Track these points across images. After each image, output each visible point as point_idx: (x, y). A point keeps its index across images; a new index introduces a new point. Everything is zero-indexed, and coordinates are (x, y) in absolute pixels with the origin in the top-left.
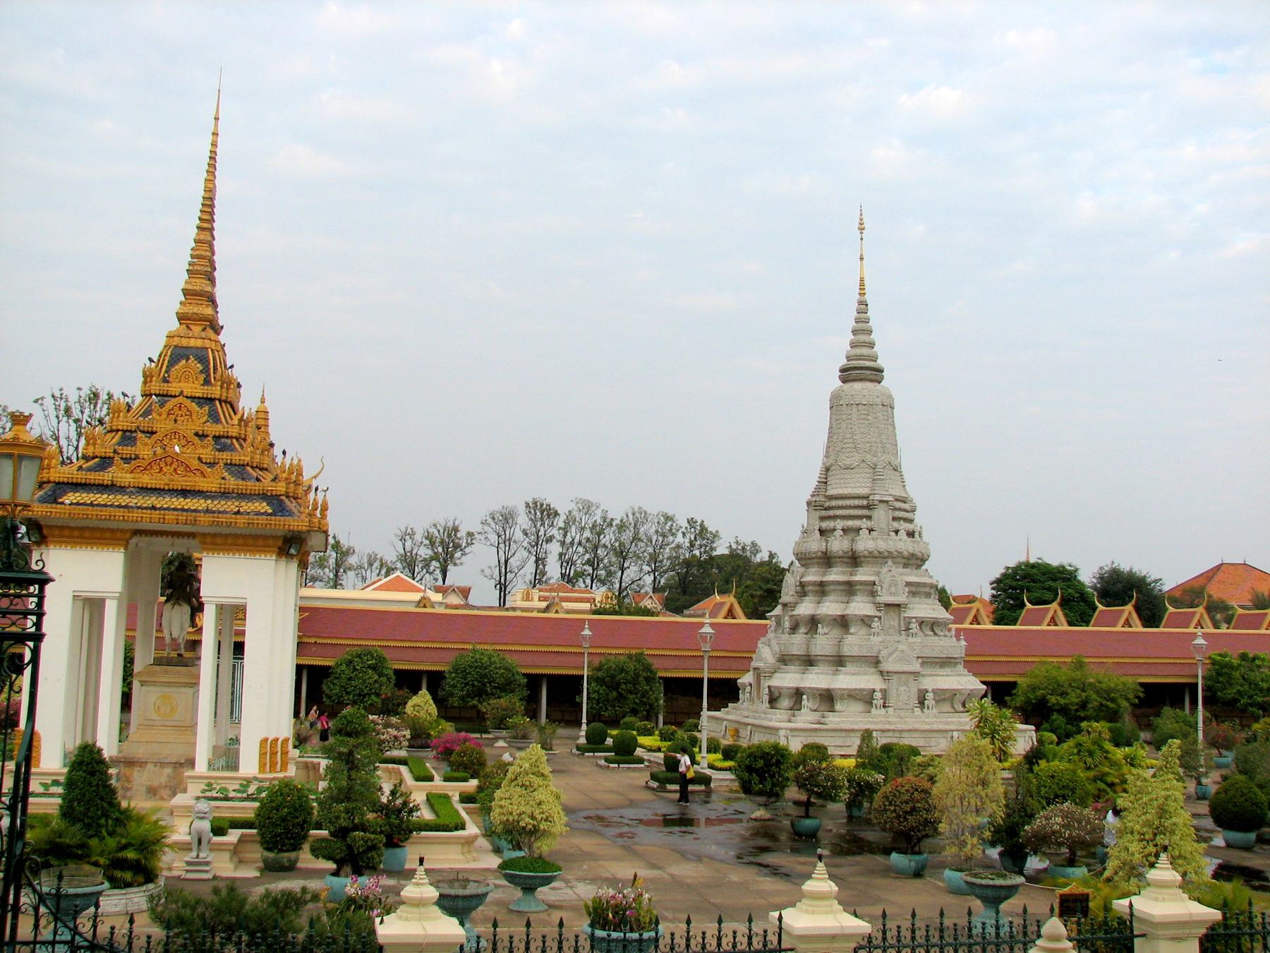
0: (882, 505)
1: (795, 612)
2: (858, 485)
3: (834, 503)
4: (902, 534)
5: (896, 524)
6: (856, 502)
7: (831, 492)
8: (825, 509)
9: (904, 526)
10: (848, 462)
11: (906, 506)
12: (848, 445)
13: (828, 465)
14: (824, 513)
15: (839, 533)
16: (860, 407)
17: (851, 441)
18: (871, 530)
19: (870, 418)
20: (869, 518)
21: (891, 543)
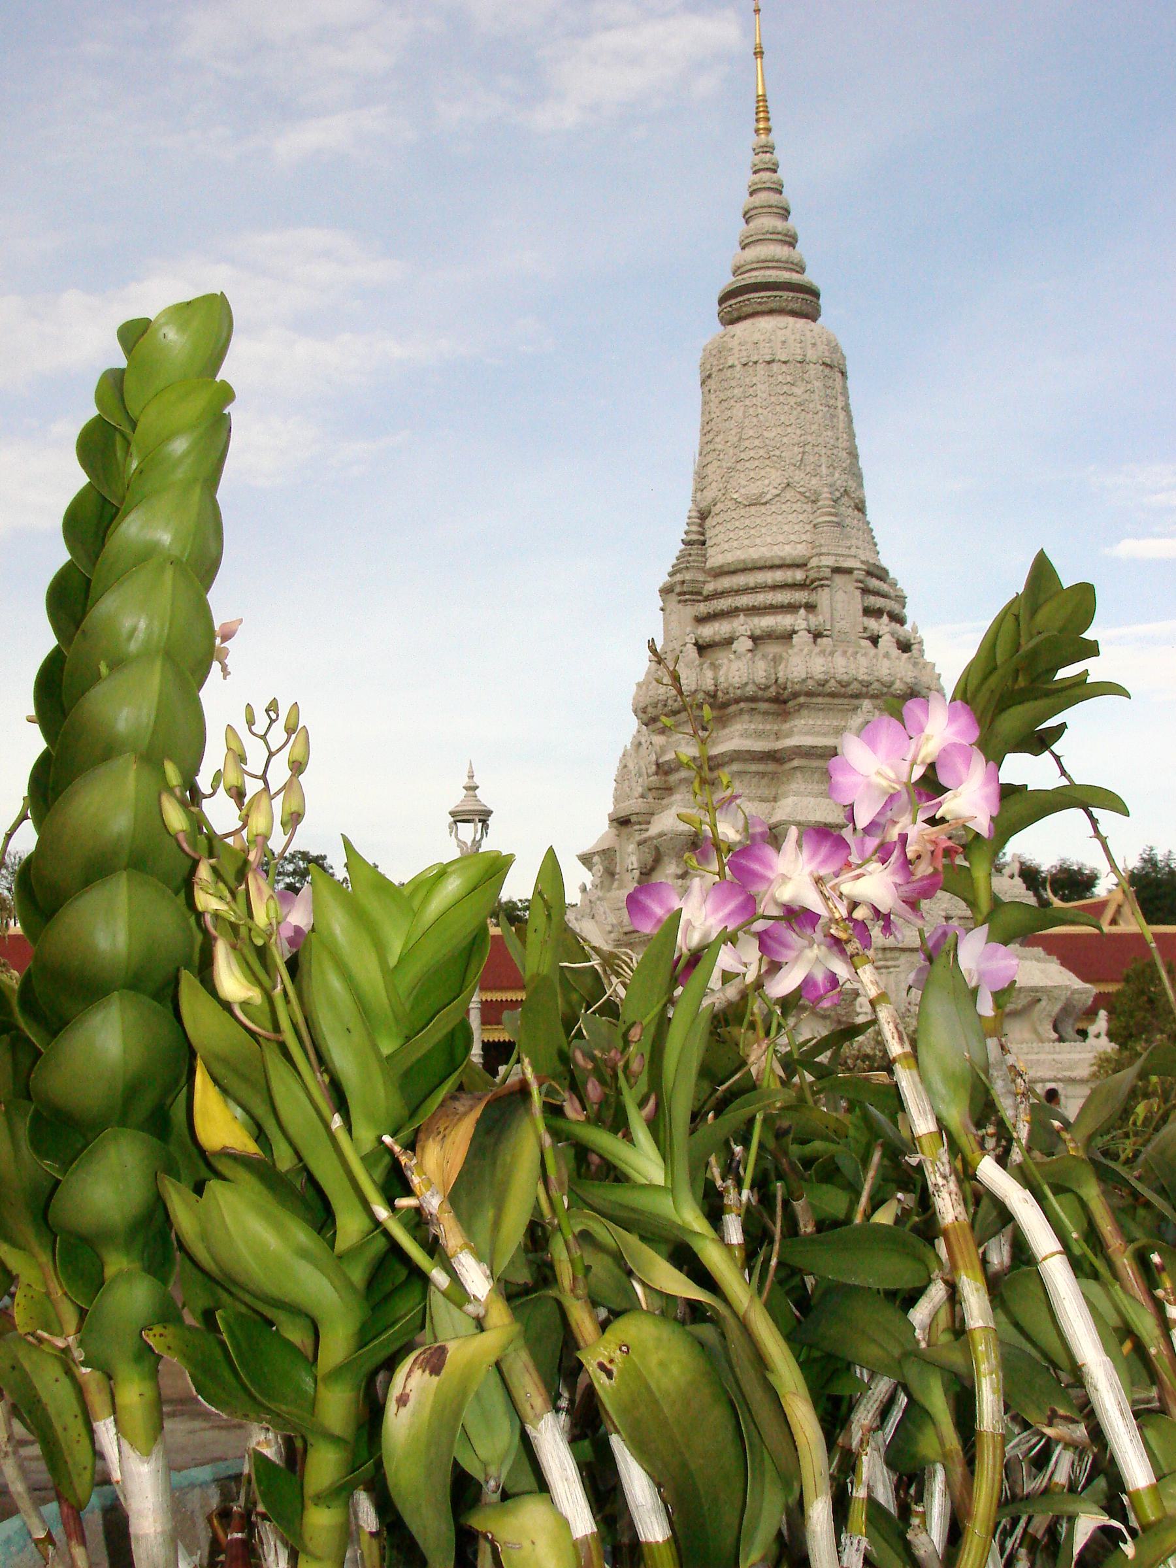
0: (839, 579)
1: (654, 830)
2: (781, 538)
3: (726, 583)
4: (886, 642)
5: (872, 623)
6: (779, 576)
7: (716, 559)
8: (707, 598)
9: (882, 626)
10: (754, 489)
11: (884, 587)
12: (752, 453)
13: (703, 505)
14: (703, 608)
15: (743, 644)
16: (775, 366)
17: (757, 442)
18: (817, 635)
19: (795, 390)
20: (811, 607)
21: (863, 661)
